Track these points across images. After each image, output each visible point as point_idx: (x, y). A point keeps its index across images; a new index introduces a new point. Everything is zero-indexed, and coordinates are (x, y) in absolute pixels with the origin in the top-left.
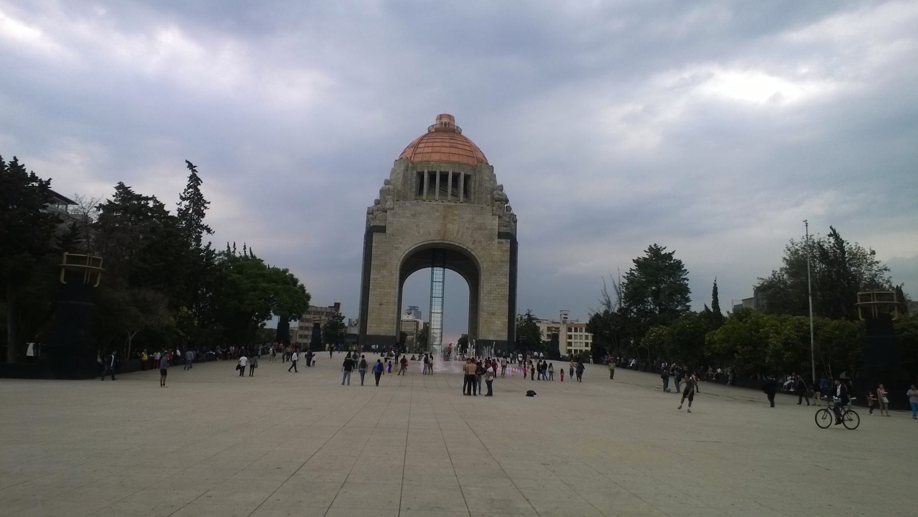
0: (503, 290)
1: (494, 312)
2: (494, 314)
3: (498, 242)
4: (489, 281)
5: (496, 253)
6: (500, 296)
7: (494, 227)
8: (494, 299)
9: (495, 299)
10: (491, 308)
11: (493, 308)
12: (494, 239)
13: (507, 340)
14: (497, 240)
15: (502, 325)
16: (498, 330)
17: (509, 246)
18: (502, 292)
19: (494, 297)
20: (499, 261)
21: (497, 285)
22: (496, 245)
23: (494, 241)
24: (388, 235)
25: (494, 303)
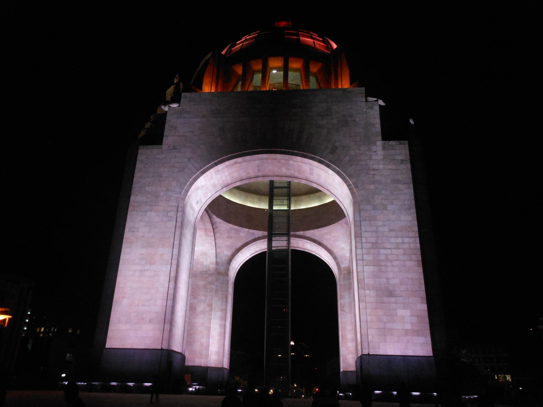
0: (406, 240)
1: (391, 288)
2: (391, 294)
3: (384, 148)
4: (373, 222)
5: (381, 167)
6: (401, 251)
7: (372, 121)
8: (387, 260)
9: (391, 261)
10: (384, 280)
11: (388, 279)
12: (375, 143)
13: (431, 354)
14: (380, 143)
15: (414, 320)
16: (406, 331)
17: (407, 152)
18: (403, 243)
19: (387, 255)
20: (389, 181)
21: (391, 230)
22: (380, 152)
23: (376, 145)
24: (164, 147)
25: (390, 269)
